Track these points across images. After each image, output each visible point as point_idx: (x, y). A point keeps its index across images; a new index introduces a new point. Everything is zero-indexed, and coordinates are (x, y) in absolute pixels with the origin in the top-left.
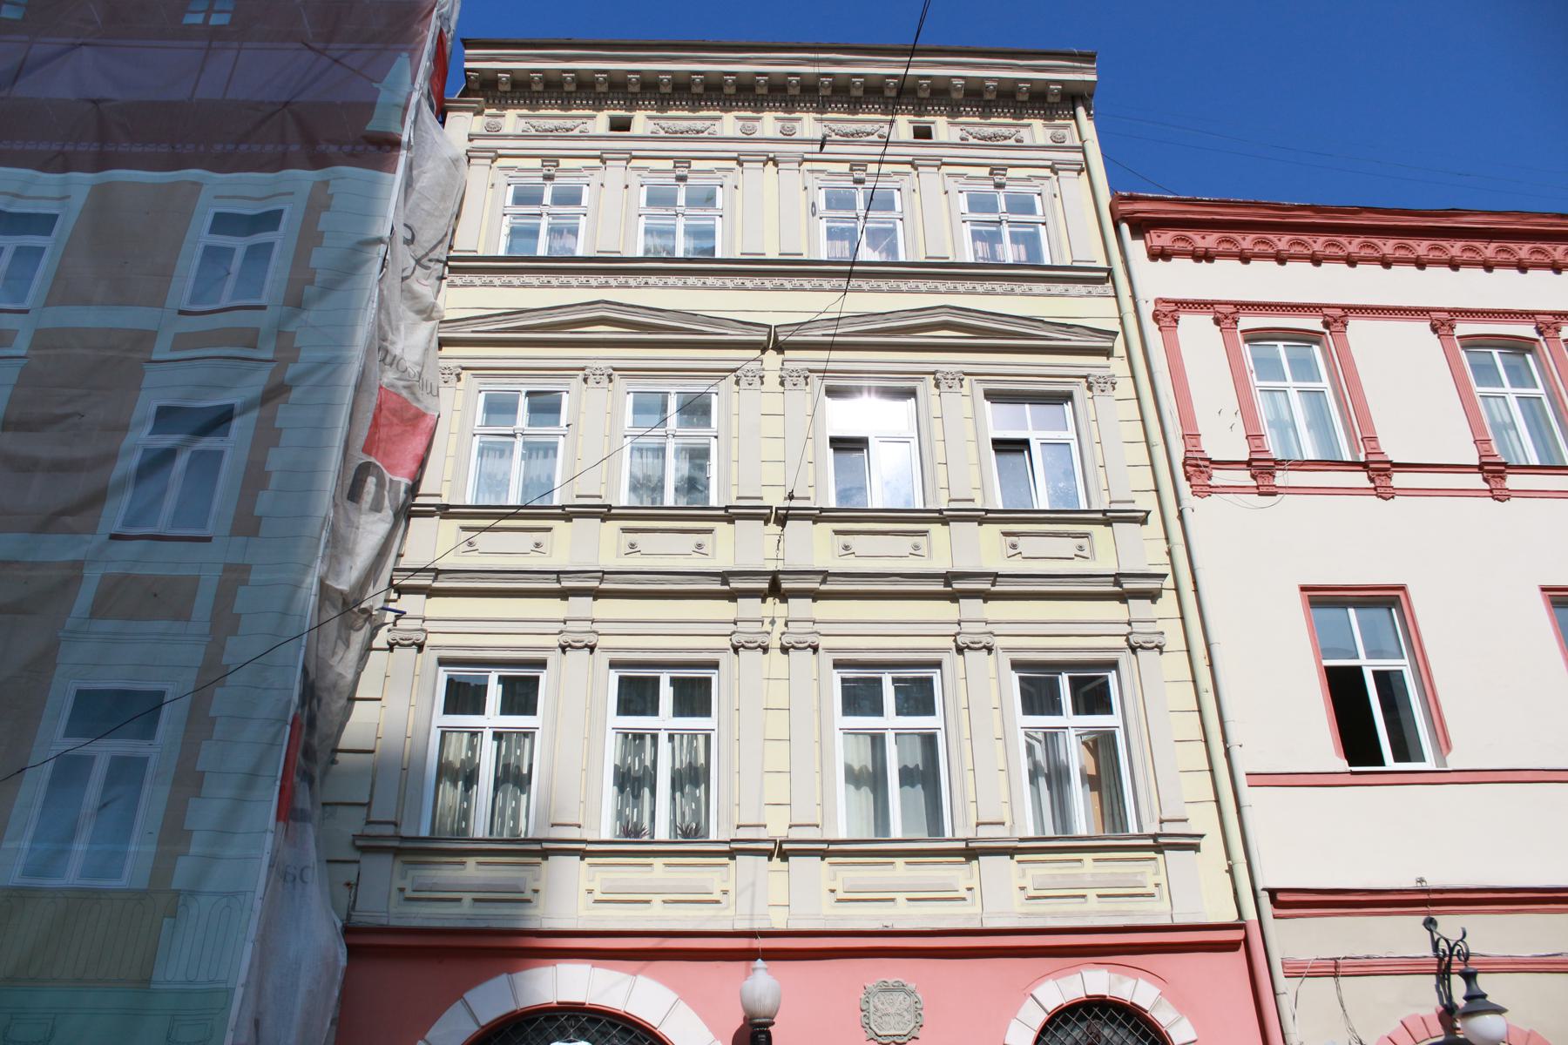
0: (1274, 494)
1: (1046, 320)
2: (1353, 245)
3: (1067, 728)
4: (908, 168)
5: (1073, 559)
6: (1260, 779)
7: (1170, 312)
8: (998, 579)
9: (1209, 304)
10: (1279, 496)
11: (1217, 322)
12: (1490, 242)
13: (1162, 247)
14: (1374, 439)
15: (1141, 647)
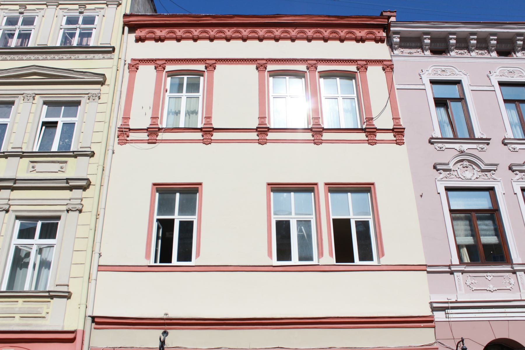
0: (155, 143)
1: (75, 70)
2: (228, 32)
3: (33, 244)
4: (104, 6)
5: (57, 172)
6: (102, 268)
7: (135, 64)
8: (17, 181)
9: (154, 60)
10: (157, 144)
11: (156, 68)
12: (296, 29)
13: (140, 36)
14: (210, 118)
15: (70, 210)
